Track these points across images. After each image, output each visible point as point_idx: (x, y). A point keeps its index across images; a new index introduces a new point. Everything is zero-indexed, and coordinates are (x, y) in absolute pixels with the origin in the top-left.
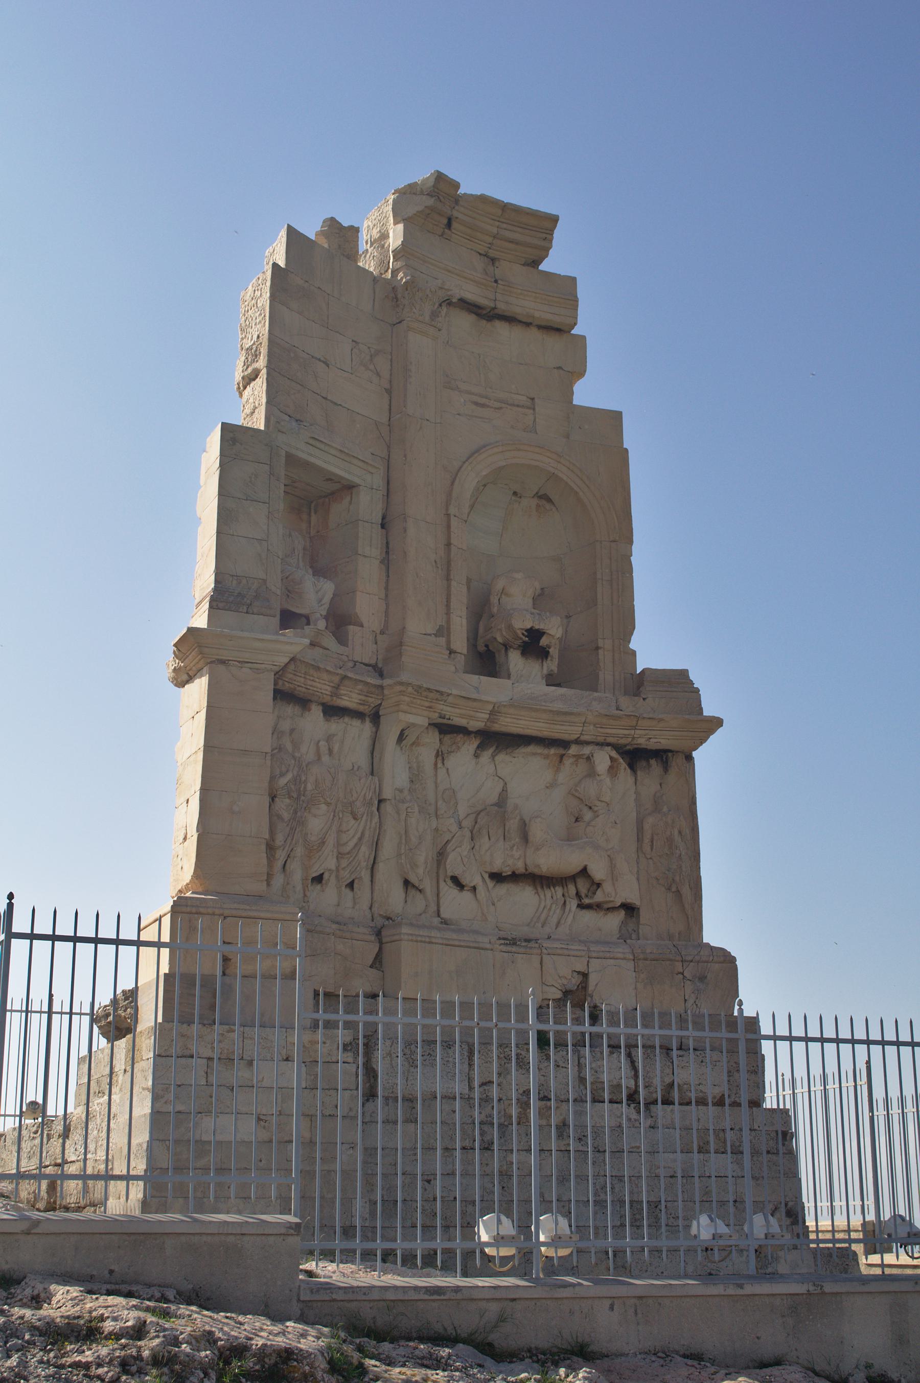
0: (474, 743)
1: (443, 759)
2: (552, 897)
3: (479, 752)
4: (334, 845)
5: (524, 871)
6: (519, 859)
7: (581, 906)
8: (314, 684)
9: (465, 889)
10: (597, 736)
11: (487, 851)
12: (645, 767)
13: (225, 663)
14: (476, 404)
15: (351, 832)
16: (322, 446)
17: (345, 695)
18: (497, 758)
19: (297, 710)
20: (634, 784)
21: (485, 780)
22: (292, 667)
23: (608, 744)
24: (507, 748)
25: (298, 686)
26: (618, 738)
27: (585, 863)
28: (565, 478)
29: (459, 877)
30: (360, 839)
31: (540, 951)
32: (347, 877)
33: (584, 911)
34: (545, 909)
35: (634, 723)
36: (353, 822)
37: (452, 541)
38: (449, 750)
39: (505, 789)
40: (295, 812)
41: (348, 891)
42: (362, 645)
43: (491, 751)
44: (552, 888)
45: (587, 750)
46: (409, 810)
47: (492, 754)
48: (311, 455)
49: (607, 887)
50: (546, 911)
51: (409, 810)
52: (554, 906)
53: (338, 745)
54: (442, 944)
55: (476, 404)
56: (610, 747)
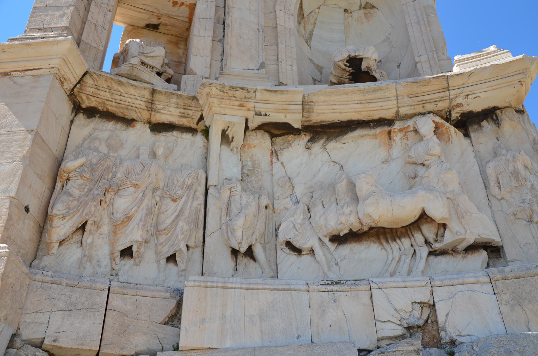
0: (304, 139)
1: (277, 156)
2: (400, 249)
3: (309, 144)
4: (141, 220)
6: (350, 214)
8: (123, 98)
9: (303, 253)
10: (414, 105)
11: (321, 216)
17: (162, 109)
18: (327, 147)
20: (471, 145)
21: (322, 166)
22: (88, 80)
23: (429, 112)
24: (336, 138)
25: (106, 100)
26: (436, 103)
29: (291, 241)
30: (177, 216)
31: (368, 287)
33: (439, 258)
35: (444, 84)
36: (172, 203)
37: (278, 22)
38: (282, 147)
40: (90, 190)
41: (171, 265)
42: (194, 85)
43: (322, 141)
44: (398, 241)
45: (410, 123)
46: (233, 189)
47: (323, 144)
49: (454, 225)
50: (394, 263)
52: (403, 257)
53: (162, 149)
54: (241, 288)
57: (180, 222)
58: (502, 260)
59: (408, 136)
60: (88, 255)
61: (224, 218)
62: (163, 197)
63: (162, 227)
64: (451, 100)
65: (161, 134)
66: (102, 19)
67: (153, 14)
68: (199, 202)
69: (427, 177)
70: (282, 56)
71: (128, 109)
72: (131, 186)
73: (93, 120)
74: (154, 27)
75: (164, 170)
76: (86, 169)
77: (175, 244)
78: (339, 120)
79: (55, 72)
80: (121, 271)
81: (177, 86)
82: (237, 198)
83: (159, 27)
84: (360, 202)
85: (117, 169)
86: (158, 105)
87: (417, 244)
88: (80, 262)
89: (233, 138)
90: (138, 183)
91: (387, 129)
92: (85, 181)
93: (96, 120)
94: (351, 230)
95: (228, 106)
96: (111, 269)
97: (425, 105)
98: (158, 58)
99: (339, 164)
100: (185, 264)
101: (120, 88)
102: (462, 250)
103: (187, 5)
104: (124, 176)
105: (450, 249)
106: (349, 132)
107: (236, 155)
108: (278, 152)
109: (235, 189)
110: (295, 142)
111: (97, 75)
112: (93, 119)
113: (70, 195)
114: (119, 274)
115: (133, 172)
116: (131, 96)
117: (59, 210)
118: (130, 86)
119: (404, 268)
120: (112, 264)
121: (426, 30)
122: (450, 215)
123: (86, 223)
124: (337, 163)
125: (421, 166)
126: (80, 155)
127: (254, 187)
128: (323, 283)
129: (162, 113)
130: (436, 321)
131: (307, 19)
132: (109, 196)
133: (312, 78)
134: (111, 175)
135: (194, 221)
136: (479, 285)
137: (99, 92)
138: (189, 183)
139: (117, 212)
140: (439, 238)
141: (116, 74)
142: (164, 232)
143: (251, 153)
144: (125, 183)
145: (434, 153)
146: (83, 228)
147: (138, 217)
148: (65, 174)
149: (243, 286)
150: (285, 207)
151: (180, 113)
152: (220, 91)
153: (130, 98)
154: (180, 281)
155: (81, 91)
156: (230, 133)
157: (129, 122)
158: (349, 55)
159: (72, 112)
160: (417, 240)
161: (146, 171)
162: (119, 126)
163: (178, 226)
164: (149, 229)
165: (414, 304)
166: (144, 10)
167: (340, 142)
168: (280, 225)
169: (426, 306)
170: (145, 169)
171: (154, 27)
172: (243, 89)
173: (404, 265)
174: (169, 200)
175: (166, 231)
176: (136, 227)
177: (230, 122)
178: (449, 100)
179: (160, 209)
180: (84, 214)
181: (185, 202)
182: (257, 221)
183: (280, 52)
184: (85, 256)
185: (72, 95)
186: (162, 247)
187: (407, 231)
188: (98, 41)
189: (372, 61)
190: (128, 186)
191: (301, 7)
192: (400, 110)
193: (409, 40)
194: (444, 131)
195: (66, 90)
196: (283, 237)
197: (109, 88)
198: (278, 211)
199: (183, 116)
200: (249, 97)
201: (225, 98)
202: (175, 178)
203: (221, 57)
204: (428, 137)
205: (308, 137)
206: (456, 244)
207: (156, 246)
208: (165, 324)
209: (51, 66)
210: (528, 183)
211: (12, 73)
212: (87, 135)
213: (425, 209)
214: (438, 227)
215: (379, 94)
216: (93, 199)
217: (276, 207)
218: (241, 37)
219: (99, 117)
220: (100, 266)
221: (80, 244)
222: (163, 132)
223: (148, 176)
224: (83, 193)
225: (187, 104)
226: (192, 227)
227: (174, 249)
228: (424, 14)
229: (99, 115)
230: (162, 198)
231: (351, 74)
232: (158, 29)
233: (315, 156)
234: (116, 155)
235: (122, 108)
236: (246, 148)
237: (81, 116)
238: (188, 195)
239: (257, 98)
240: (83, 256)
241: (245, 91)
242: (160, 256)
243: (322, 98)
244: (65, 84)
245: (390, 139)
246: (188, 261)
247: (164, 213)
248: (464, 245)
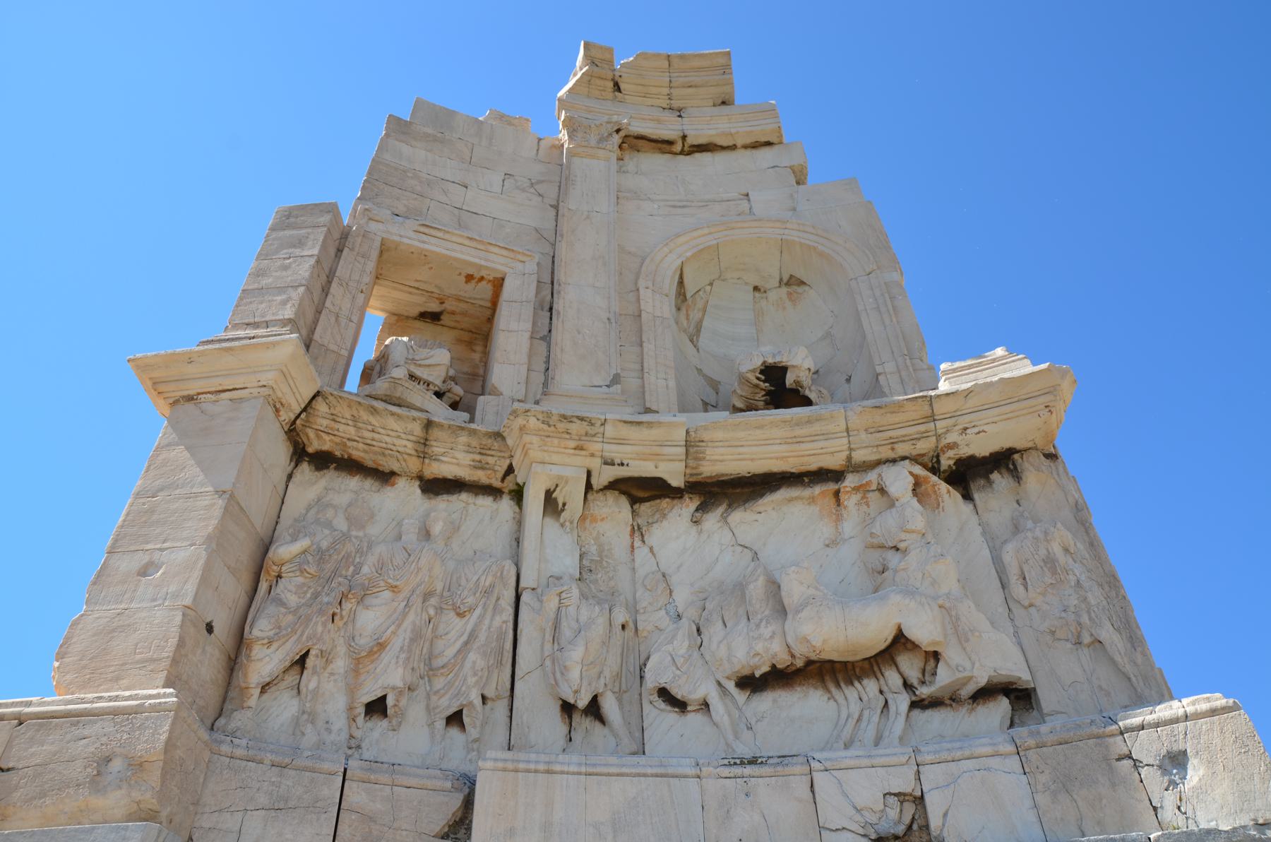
0: (689, 505)
1: (642, 535)
2: (861, 699)
3: (698, 515)
4: (402, 648)
6: (772, 637)
7: (917, 704)
9: (689, 708)
10: (877, 446)
11: (721, 642)
12: (983, 486)
14: (674, 207)
16: (440, 234)
17: (443, 454)
18: (730, 519)
19: (377, 484)
21: (720, 553)
22: (321, 406)
23: (904, 458)
24: (744, 504)
25: (348, 439)
26: (914, 442)
28: (797, 239)
29: (668, 688)
30: (466, 643)
31: (806, 769)
33: (929, 713)
34: (850, 720)
36: (457, 620)
37: (642, 307)
38: (650, 521)
40: (316, 595)
41: (454, 732)
43: (721, 510)
44: (857, 684)
45: (872, 476)
46: (564, 595)
47: (722, 515)
48: (424, 242)
49: (952, 655)
50: (852, 723)
52: (866, 713)
53: (441, 523)
55: (674, 207)
57: (471, 653)
58: (1035, 713)
59: (869, 499)
60: (309, 711)
61: (548, 646)
62: (441, 608)
63: (439, 662)
64: (938, 437)
65: (440, 498)
66: (349, 306)
67: (433, 295)
68: (505, 618)
69: (903, 569)
70: (649, 363)
71: (384, 455)
72: (385, 588)
74: (432, 317)
75: (443, 561)
76: (310, 558)
77: (462, 693)
78: (749, 473)
79: (268, 393)
80: (367, 740)
81: (468, 415)
82: (572, 610)
83: (442, 317)
84: (790, 616)
86: (437, 448)
87: (890, 689)
88: (296, 722)
89: (564, 505)
90: (398, 583)
91: (832, 486)
92: (308, 580)
93: (330, 474)
94: (774, 666)
95: (556, 449)
96: (348, 737)
97: (896, 446)
98: (438, 368)
99: (751, 550)
100: (478, 729)
101: (372, 419)
102: (966, 697)
103: (490, 281)
104: (374, 570)
105: (947, 696)
106: (767, 494)
108: (644, 529)
109: (569, 595)
110: (674, 511)
111: (335, 398)
112: (325, 471)
113: (281, 603)
114: (363, 745)
115: (390, 565)
116: (391, 433)
117: (262, 631)
118: (389, 415)
119: (869, 733)
120: (350, 727)
121: (892, 321)
122: (945, 636)
123: (308, 652)
124: (746, 547)
125: (892, 552)
126: (301, 535)
127: (601, 591)
128: (726, 762)
129: (442, 461)
130: (926, 827)
131: (692, 303)
132: (347, 606)
133: (702, 400)
134: (352, 568)
135: (495, 652)
136: (997, 759)
137: (336, 426)
138: (487, 584)
139: (360, 635)
140: (927, 678)
141: (367, 396)
142: (442, 671)
143: (596, 532)
144: (375, 584)
145: (914, 528)
146: (301, 662)
147: (397, 643)
148: (275, 568)
149: (583, 769)
150: (657, 627)
151: (473, 461)
152: (543, 422)
153: (388, 435)
155: (307, 425)
156: (559, 496)
157: (385, 477)
158: (764, 362)
159: (291, 460)
160: (890, 682)
161: (413, 562)
162: (369, 483)
163: (467, 660)
164: (416, 665)
165: (888, 796)
166: (418, 289)
167: (752, 510)
168: (648, 658)
169: (908, 800)
170: (412, 558)
171: (432, 317)
172: (582, 419)
174: (452, 614)
175: (446, 670)
176: (394, 661)
177: (560, 477)
178: (935, 438)
179: (436, 629)
181: (478, 618)
182: (608, 651)
183: (645, 356)
184: (304, 712)
185: (292, 432)
186: (439, 699)
187: (872, 666)
188: (339, 340)
189: (803, 371)
190: (381, 589)
191: (681, 282)
192: (854, 454)
193: (864, 337)
194: (930, 490)
195: (283, 423)
197: (355, 419)
198: (645, 634)
199: (481, 466)
201: (551, 434)
202: (463, 575)
204: (903, 500)
206: (957, 688)
207: (428, 697)
208: (443, 838)
209: (261, 384)
210: (1071, 577)
212: (313, 500)
213: (902, 627)
214: (926, 658)
215: (817, 428)
216: (321, 612)
217: (640, 627)
218: (579, 333)
219: (336, 469)
220: (329, 731)
221: (295, 691)
222: (442, 494)
223: (416, 570)
224: (303, 601)
225: (485, 445)
226: (491, 662)
227: (459, 701)
228: (886, 295)
229: (334, 465)
230: (439, 610)
231: (768, 393)
232: (439, 319)
233: (709, 536)
234: (361, 534)
235: (375, 453)
236: (588, 521)
237: (305, 467)
239: (608, 434)
240: (301, 712)
241: (585, 423)
242: (435, 715)
243: (719, 435)
244: (281, 413)
245: (839, 505)
246: (485, 723)
247: (443, 637)
248: (971, 689)
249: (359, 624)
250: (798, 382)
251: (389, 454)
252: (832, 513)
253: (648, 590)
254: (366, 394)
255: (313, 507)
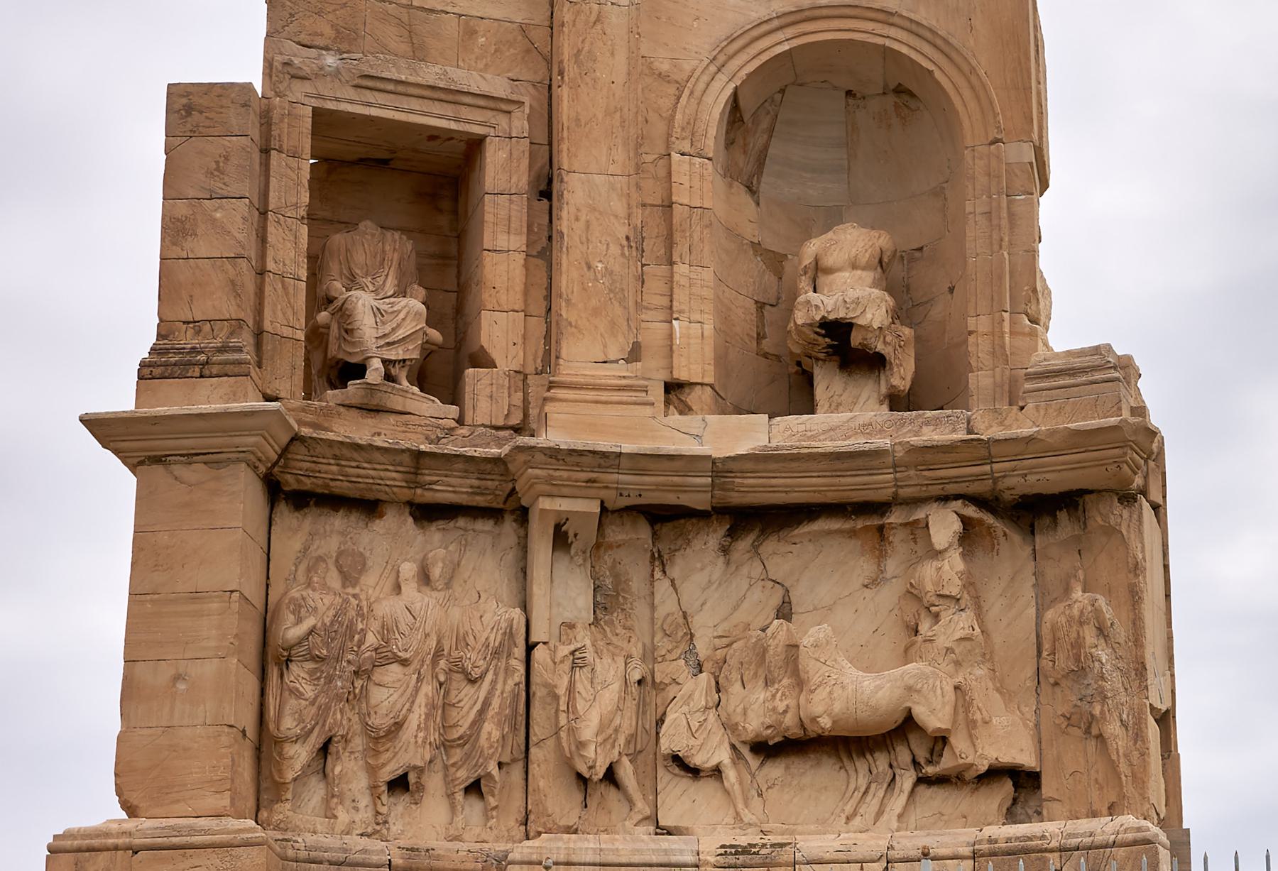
4: (419, 726)
5: (800, 733)
6: (785, 712)
9: (701, 774)
10: (927, 485)
13: (161, 461)
15: (466, 704)
16: (391, 87)
17: (435, 483)
21: (748, 589)
24: (779, 531)
25: (332, 479)
26: (967, 484)
27: (908, 704)
29: (680, 754)
30: (482, 712)
32: (464, 776)
36: (469, 687)
37: (674, 199)
38: (672, 547)
39: (787, 599)
42: (491, 397)
45: (920, 514)
46: (578, 655)
49: (959, 743)
51: (578, 655)
53: (440, 565)
56: (960, 501)
57: (486, 724)
60: (338, 794)
63: (455, 734)
65: (433, 527)
68: (517, 679)
70: (680, 297)
73: (306, 514)
85: (365, 622)
89: (576, 535)
90: (408, 656)
91: (876, 521)
94: (785, 737)
96: (374, 813)
99: (783, 586)
101: (356, 455)
104: (380, 639)
107: (582, 568)
108: (666, 557)
113: (298, 695)
114: (390, 820)
116: (378, 466)
120: (375, 805)
122: (954, 722)
131: (753, 123)
134: (357, 637)
138: (497, 644)
139: (376, 713)
141: (339, 405)
142: (459, 742)
146: (324, 750)
150: (674, 680)
151: (471, 487)
154: (491, 828)
156: (569, 528)
157: (369, 507)
158: (824, 317)
162: (354, 517)
173: (872, 802)
176: (413, 740)
179: (448, 694)
180: (327, 728)
184: (333, 796)
187: (885, 741)
192: (901, 491)
196: (666, 746)
197: (335, 457)
198: (662, 686)
200: (607, 465)
203: (545, 303)
205: (722, 531)
207: (446, 767)
211: (168, 458)
218: (589, 267)
219: (317, 504)
221: (321, 775)
222: (437, 519)
223: (424, 637)
229: (314, 499)
233: (737, 567)
234: (357, 591)
236: (602, 549)
238: (496, 666)
242: (454, 787)
249: (373, 702)
250: (865, 345)
251: (377, 490)
252: (875, 548)
253: (666, 634)
254: (338, 402)
255: (302, 560)
